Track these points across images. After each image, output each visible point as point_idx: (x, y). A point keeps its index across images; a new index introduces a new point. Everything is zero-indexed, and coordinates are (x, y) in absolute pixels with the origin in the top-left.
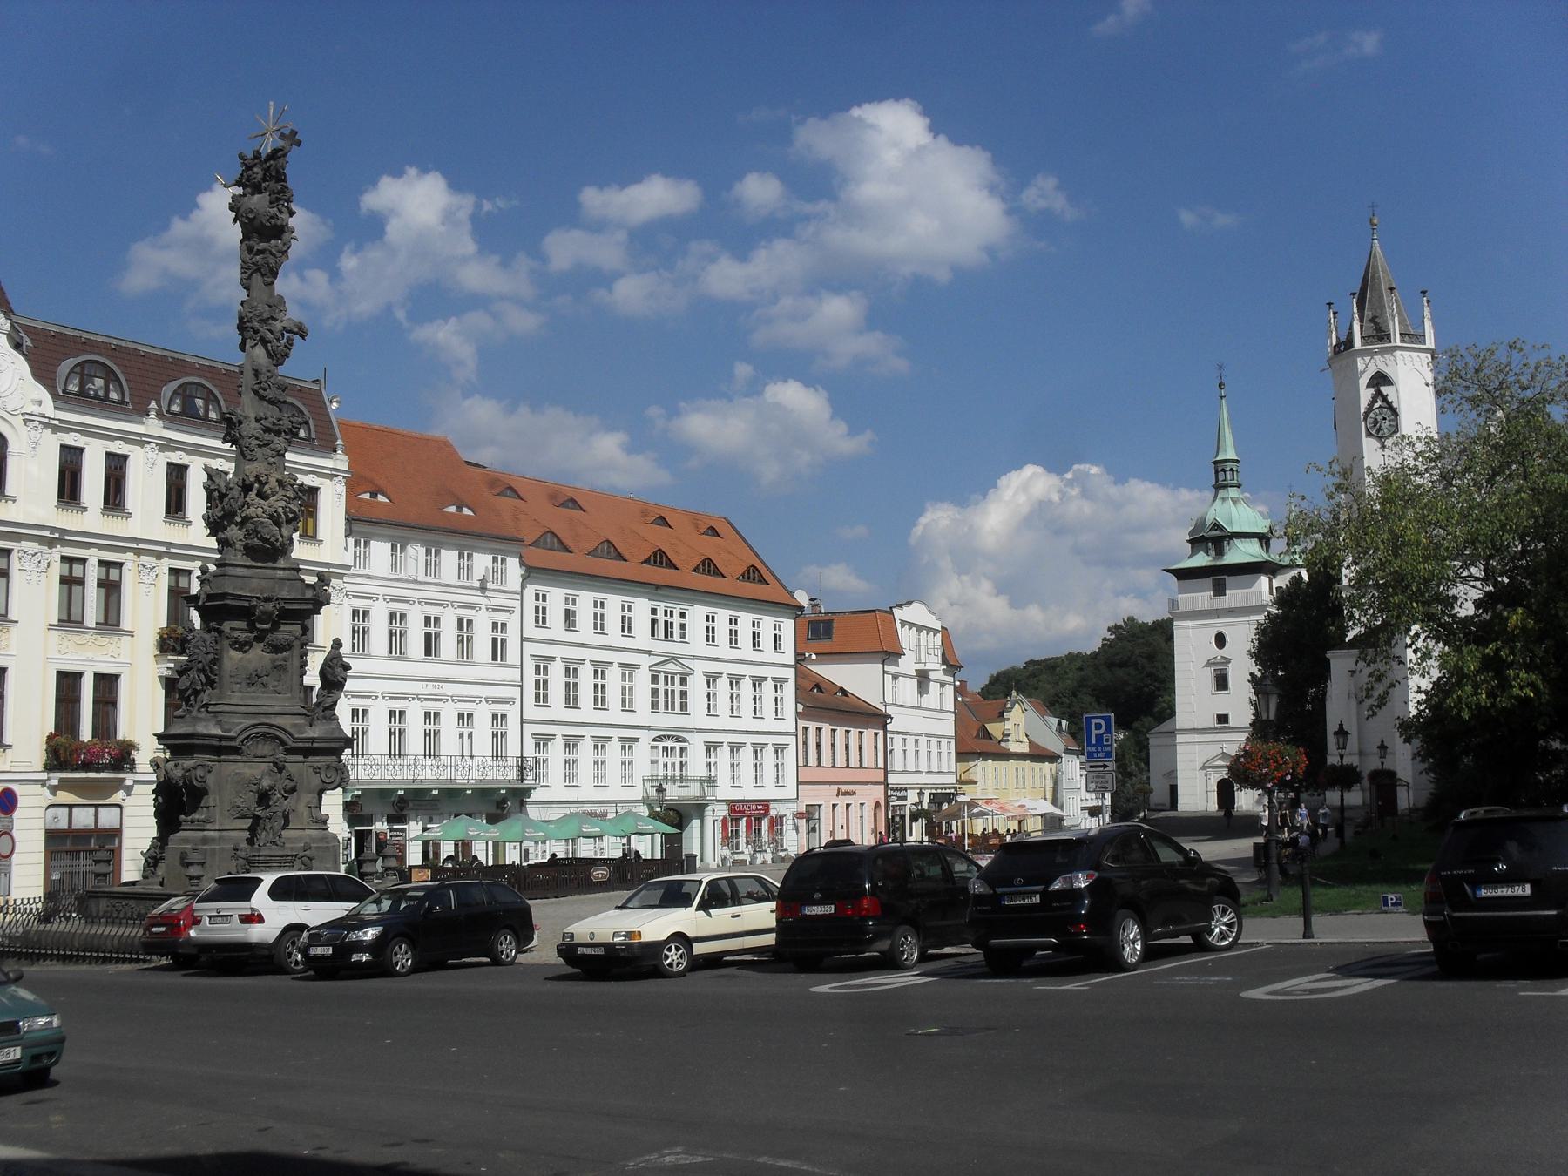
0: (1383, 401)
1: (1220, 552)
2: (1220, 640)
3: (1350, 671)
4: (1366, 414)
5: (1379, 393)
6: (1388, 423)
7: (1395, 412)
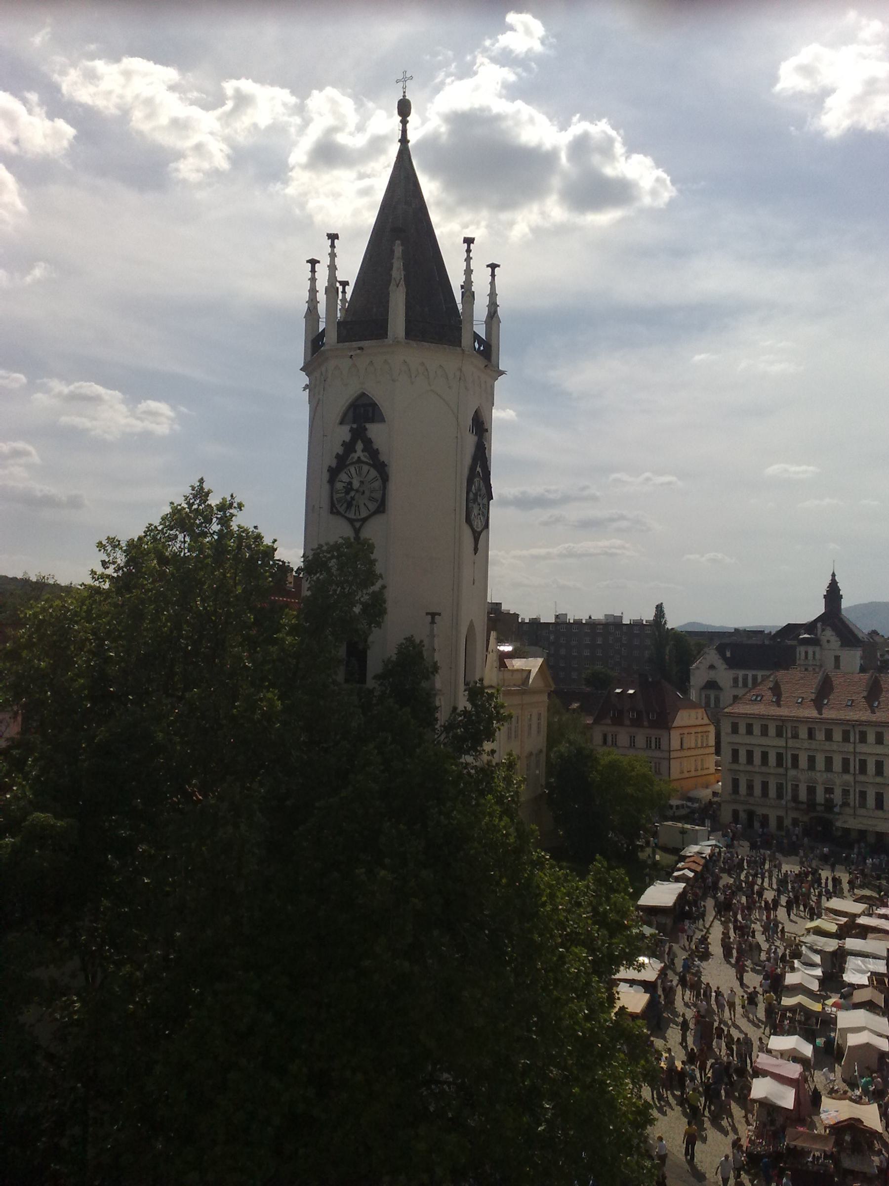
7: (382, 469)
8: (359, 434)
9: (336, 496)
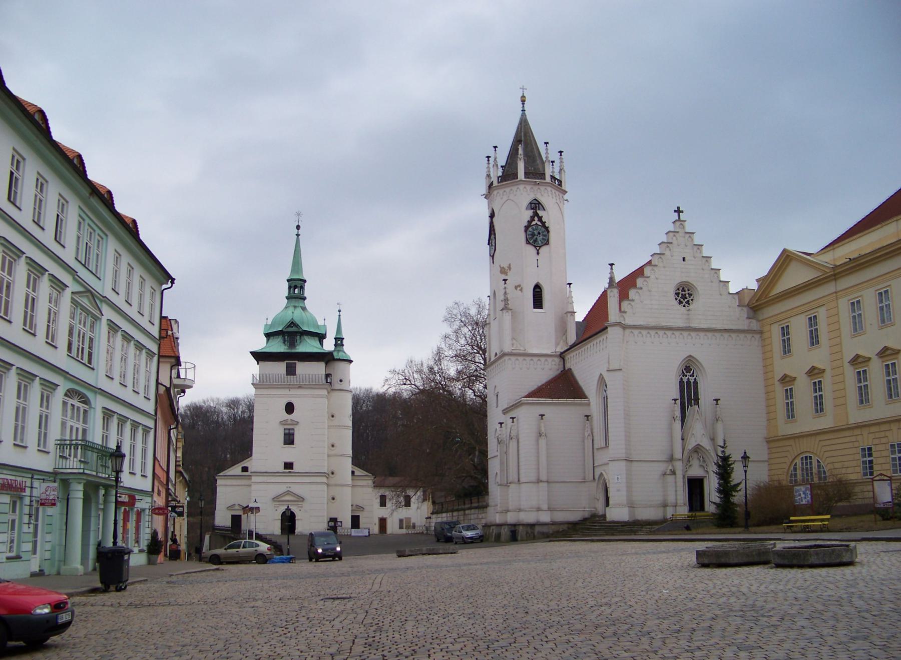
0: (538, 221)
1: (292, 344)
2: (290, 408)
3: (540, 415)
4: (527, 228)
5: (537, 214)
6: (541, 237)
7: (547, 229)
8: (536, 214)
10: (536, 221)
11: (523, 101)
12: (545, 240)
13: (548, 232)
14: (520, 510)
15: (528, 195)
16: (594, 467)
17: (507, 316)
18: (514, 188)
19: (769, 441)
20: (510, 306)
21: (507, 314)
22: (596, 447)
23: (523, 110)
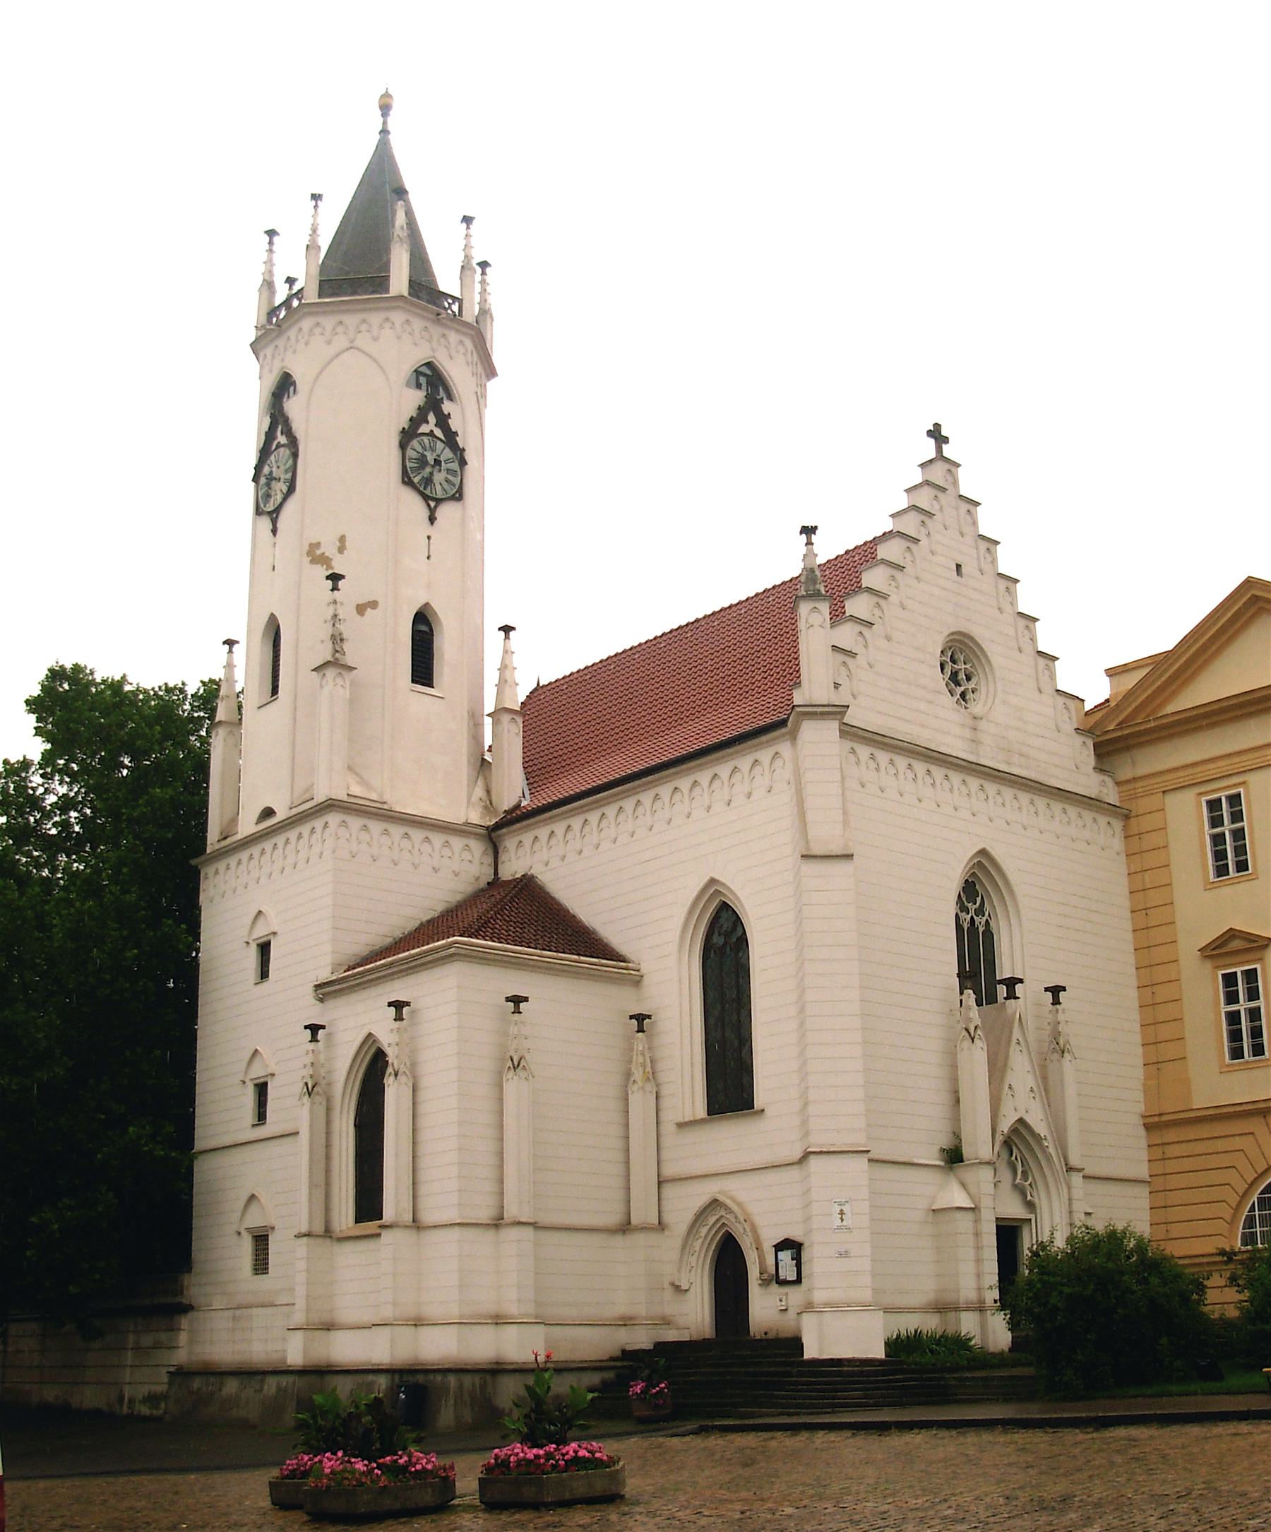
3: (508, 999)
4: (407, 436)
6: (443, 475)
8: (432, 405)
9: (408, 464)
10: (430, 425)
11: (385, 109)
12: (454, 485)
13: (463, 463)
14: (418, 1323)
15: (416, 344)
16: (659, 1183)
17: (334, 687)
18: (375, 318)
19: (1154, 1124)
20: (349, 660)
21: (339, 681)
22: (671, 1116)
23: (384, 132)
